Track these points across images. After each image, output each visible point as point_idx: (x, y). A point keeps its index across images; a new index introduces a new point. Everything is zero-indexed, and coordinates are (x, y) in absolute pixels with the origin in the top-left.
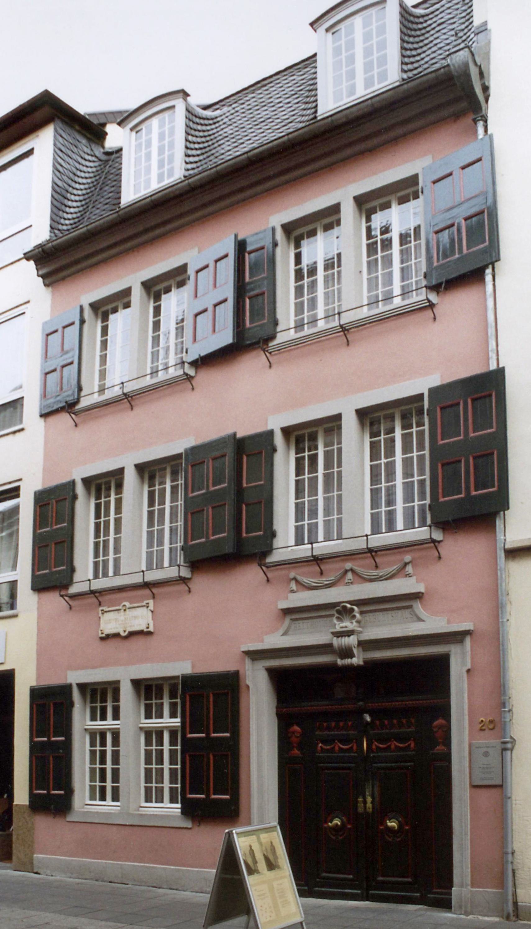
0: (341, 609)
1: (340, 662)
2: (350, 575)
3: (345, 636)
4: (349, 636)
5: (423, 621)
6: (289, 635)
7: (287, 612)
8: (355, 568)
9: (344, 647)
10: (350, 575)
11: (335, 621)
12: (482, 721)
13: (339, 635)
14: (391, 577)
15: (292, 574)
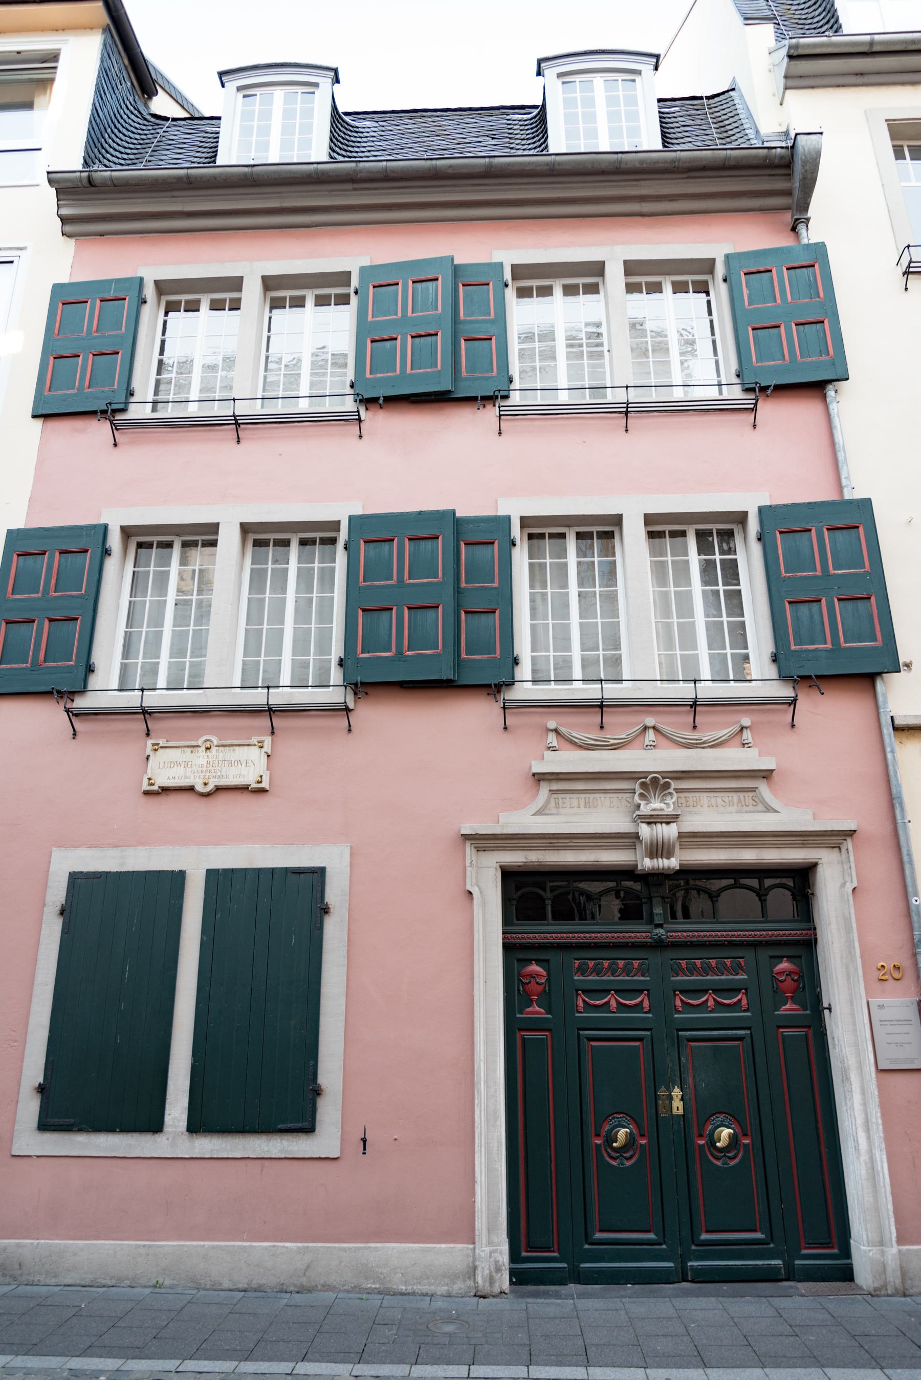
0: (649, 782)
1: (647, 864)
2: (651, 735)
3: (661, 823)
4: (668, 823)
5: (776, 812)
6: (545, 814)
7: (540, 778)
8: (659, 725)
9: (660, 840)
10: (651, 735)
11: (637, 798)
12: (883, 966)
13: (651, 820)
14: (717, 744)
15: (552, 724)
